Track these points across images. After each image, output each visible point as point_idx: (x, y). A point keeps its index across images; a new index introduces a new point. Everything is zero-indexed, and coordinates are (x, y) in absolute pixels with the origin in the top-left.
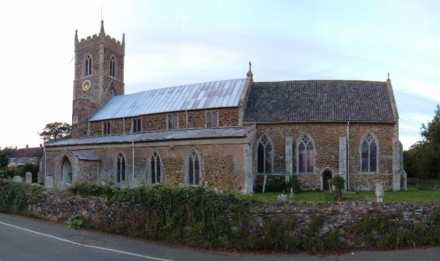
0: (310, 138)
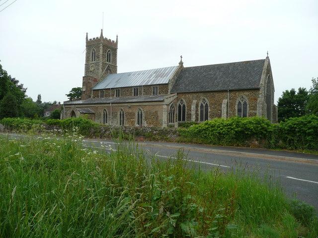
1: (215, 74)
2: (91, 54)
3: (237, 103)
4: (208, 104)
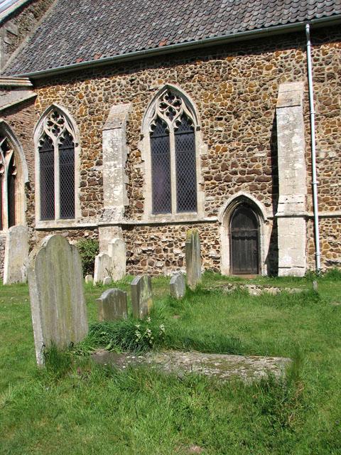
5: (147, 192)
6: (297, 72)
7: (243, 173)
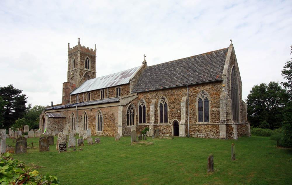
0: (166, 99)
1: (175, 70)
2: (72, 63)
3: (197, 101)
4: (167, 103)
5: (159, 118)
6: (186, 94)
7: (176, 115)
